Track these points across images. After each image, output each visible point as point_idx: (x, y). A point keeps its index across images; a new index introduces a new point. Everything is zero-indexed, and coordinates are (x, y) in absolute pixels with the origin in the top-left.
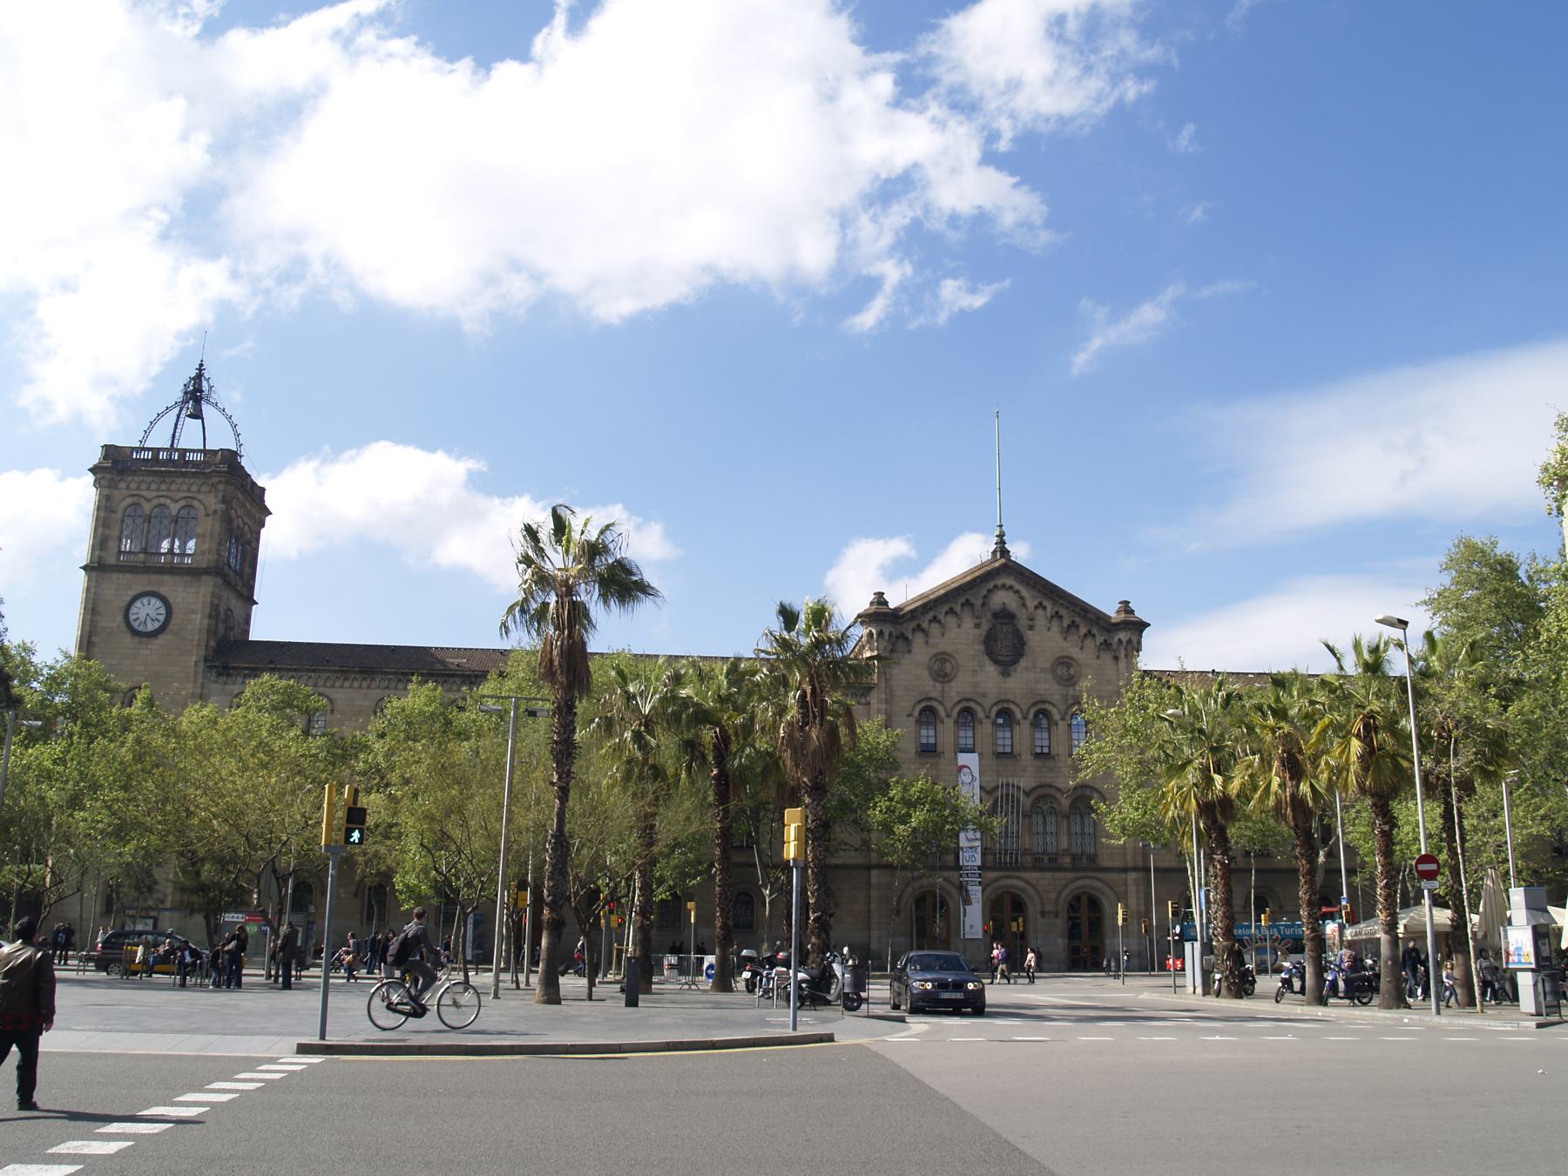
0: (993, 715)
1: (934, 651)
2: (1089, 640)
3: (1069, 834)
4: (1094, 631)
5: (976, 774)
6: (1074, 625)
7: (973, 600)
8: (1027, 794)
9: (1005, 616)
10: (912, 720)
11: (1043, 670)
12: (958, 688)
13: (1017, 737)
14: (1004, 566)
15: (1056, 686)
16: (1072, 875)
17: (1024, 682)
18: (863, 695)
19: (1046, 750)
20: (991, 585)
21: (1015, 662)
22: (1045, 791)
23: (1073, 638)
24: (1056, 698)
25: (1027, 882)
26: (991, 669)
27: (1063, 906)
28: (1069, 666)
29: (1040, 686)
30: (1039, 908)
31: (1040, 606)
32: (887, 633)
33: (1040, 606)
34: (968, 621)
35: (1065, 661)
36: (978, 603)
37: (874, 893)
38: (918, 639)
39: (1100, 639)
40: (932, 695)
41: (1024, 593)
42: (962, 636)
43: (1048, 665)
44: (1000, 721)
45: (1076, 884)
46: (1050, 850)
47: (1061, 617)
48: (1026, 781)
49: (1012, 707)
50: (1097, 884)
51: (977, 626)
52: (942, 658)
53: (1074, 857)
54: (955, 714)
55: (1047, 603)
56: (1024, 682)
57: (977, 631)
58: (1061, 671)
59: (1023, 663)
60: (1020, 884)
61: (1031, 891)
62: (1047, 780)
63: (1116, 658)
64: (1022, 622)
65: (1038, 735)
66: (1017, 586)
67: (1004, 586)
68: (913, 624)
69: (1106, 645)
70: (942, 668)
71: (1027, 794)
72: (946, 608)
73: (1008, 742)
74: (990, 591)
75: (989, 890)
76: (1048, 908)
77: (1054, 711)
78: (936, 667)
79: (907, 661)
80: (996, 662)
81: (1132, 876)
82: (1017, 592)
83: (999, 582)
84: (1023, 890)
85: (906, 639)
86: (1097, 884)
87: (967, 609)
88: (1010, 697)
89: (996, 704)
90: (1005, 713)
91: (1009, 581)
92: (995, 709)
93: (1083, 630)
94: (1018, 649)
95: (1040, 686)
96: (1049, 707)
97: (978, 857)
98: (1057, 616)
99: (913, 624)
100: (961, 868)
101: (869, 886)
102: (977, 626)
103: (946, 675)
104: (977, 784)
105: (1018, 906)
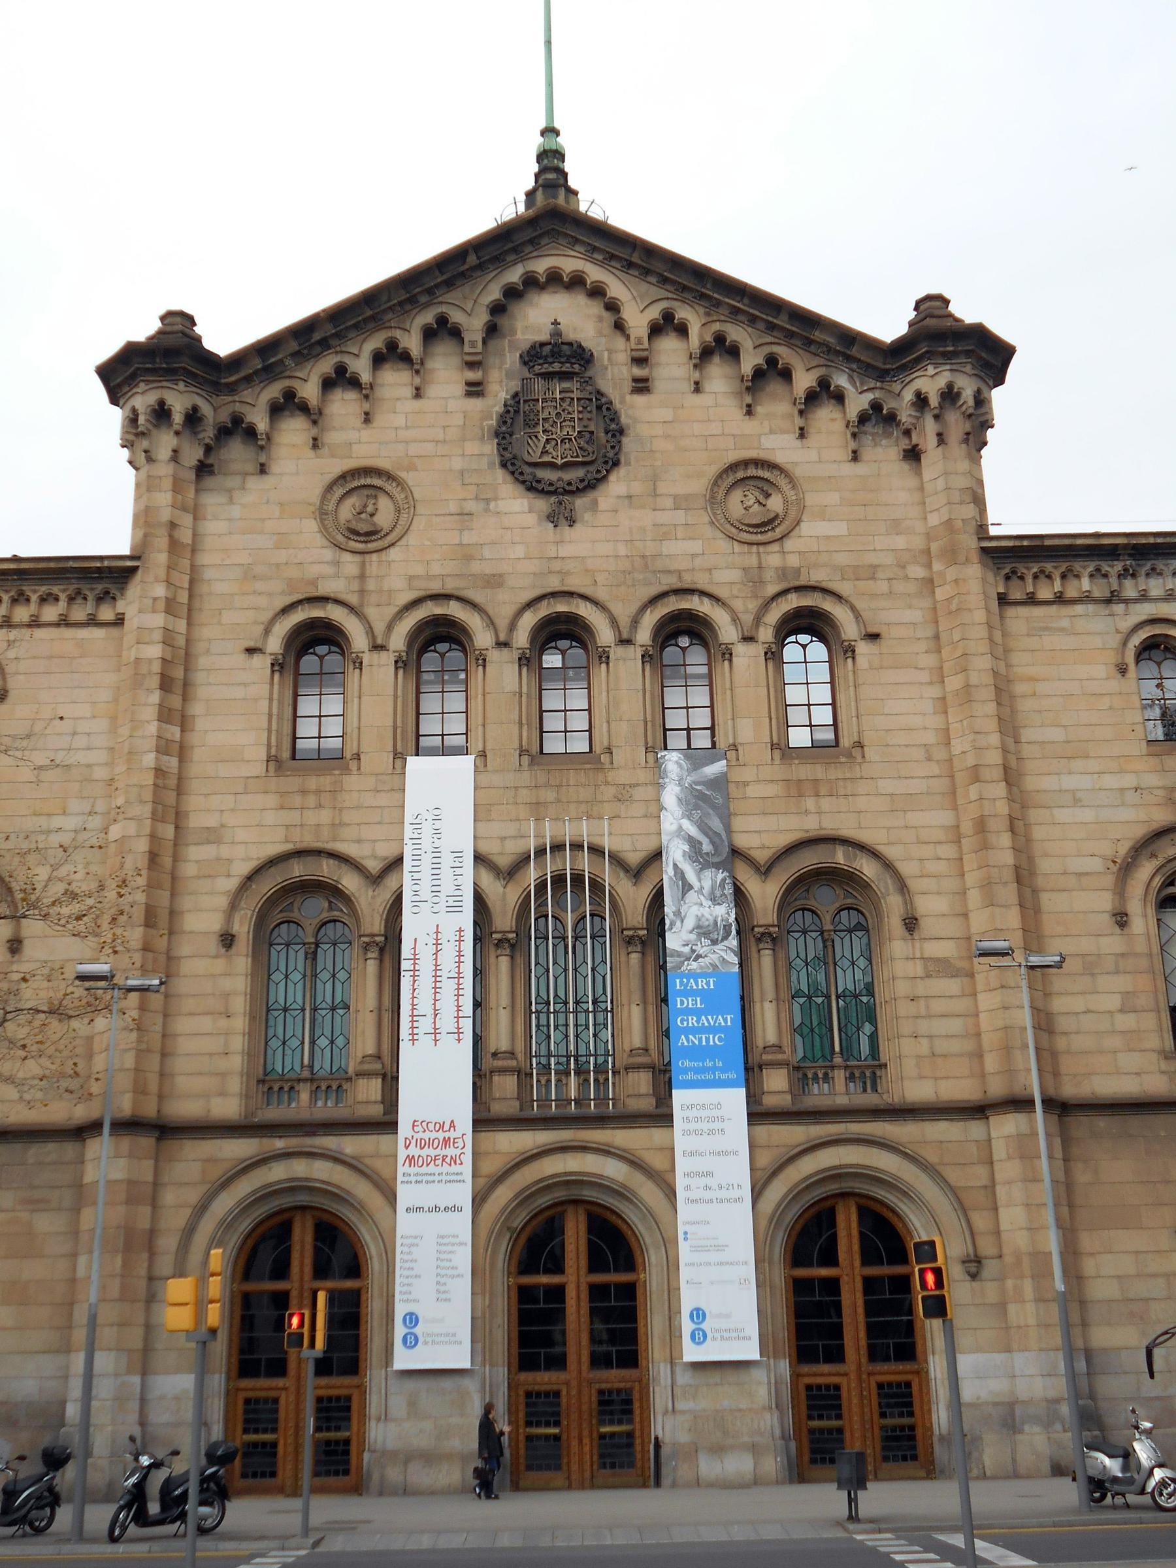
0: (522, 638)
4: (841, 380)
6: (772, 372)
7: (456, 317)
9: (561, 359)
10: (262, 663)
11: (680, 502)
12: (408, 569)
13: (600, 700)
15: (724, 545)
18: (105, 597)
21: (590, 485)
23: (777, 407)
25: (635, 1163)
26: (518, 508)
28: (766, 488)
29: (672, 547)
31: (665, 325)
33: (665, 325)
35: (752, 473)
39: (858, 402)
41: (616, 288)
43: (699, 486)
44: (552, 660)
45: (809, 1165)
47: (733, 352)
49: (584, 610)
51: (475, 389)
52: (365, 481)
54: (398, 641)
57: (475, 404)
58: (739, 504)
59: (617, 485)
60: (613, 1169)
63: (913, 455)
64: (613, 372)
66: (595, 273)
67: (554, 279)
68: (274, 391)
69: (877, 417)
72: (376, 342)
73: (579, 722)
74: (513, 294)
77: (719, 617)
78: (346, 511)
80: (533, 487)
81: (1006, 1126)
82: (597, 292)
83: (541, 266)
85: (251, 433)
88: (575, 583)
89: (530, 604)
91: (569, 263)
92: (529, 620)
93: (804, 380)
95: (672, 547)
96: (703, 606)
98: (720, 348)
99: (274, 391)
101: (80, 1194)
102: (475, 389)
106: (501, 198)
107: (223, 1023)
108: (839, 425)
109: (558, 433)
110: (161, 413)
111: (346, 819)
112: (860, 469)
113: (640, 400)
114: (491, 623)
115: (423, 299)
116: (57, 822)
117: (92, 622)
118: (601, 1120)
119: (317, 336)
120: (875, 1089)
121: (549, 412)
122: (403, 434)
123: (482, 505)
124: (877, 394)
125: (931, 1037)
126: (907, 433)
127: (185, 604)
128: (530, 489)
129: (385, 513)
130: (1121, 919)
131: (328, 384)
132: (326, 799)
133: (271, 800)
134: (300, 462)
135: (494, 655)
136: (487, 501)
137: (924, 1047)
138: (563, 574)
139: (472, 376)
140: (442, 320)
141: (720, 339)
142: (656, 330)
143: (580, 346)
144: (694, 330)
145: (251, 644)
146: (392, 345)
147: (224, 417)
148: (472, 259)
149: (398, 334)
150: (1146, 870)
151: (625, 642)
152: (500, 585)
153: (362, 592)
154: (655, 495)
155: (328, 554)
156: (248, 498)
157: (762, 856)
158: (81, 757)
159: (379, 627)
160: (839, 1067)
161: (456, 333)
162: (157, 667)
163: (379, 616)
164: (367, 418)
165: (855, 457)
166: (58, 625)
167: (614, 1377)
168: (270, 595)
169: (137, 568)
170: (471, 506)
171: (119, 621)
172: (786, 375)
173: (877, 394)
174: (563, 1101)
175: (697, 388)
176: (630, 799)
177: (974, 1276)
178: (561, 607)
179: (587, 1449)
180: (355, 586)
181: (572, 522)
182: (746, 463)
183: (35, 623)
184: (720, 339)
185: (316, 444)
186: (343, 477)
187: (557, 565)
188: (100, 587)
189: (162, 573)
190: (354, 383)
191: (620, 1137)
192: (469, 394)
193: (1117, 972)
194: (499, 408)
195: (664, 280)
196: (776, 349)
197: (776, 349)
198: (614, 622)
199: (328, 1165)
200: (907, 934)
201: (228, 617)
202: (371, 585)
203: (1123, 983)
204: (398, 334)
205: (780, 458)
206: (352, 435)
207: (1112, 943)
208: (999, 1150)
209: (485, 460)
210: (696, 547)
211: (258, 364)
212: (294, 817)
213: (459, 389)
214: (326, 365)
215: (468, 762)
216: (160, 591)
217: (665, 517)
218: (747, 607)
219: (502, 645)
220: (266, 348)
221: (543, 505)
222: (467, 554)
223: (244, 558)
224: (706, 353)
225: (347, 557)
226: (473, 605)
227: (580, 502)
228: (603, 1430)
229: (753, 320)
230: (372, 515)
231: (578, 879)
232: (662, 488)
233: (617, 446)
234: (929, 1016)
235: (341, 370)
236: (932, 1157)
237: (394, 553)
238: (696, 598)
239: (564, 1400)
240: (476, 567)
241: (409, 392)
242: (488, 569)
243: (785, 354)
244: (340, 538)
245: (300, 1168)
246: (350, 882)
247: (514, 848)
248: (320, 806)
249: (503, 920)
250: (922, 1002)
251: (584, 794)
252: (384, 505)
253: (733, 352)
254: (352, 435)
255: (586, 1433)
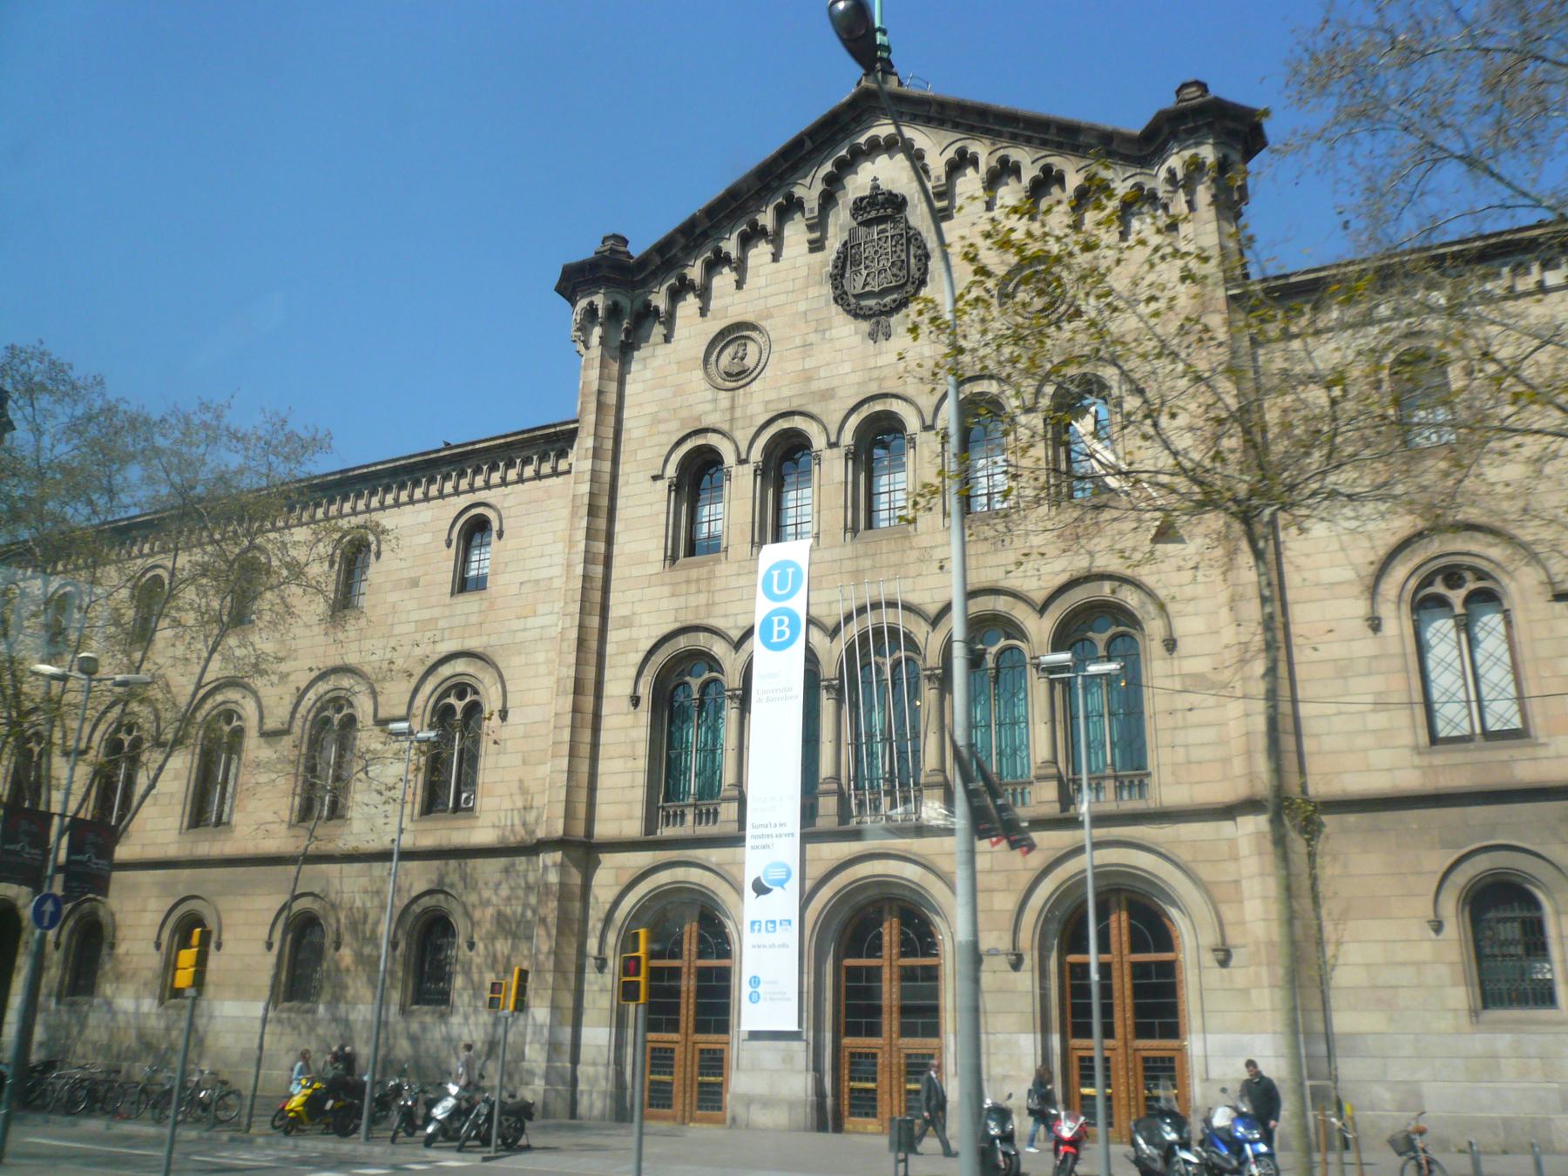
9: (883, 207)
10: (663, 485)
26: (847, 331)
30: (1209, 937)
35: (1035, 269)
47: (1013, 170)
49: (896, 406)
51: (816, 246)
52: (735, 333)
57: (818, 256)
60: (910, 872)
80: (857, 314)
107: (631, 764)
109: (876, 267)
110: (591, 311)
111: (717, 599)
115: (775, 184)
116: (531, 622)
117: (555, 473)
119: (698, 231)
120: (1141, 795)
121: (870, 251)
122: (764, 292)
123: (820, 335)
124: (1138, 179)
125: (1186, 746)
126: (1165, 207)
127: (611, 450)
128: (856, 316)
130: (1375, 624)
132: (703, 585)
133: (666, 590)
134: (692, 327)
136: (824, 331)
137: (1180, 755)
138: (881, 380)
143: (890, 193)
145: (655, 473)
147: (638, 304)
148: (808, 144)
150: (1400, 572)
152: (833, 397)
153: (732, 420)
155: (709, 395)
156: (657, 362)
157: (1039, 597)
158: (544, 574)
159: (743, 447)
160: (1108, 777)
162: (586, 500)
166: (533, 479)
167: (1155, 1046)
168: (668, 432)
169: (576, 429)
170: (813, 338)
172: (1060, 180)
173: (1138, 179)
176: (931, 559)
177: (1224, 963)
178: (878, 407)
179: (896, 1102)
180: (728, 417)
181: (888, 336)
183: (521, 480)
186: (722, 334)
187: (875, 374)
188: (557, 446)
189: (592, 430)
192: (812, 250)
193: (1369, 674)
194: (834, 256)
196: (1050, 160)
197: (1050, 160)
199: (699, 871)
200: (1166, 654)
201: (641, 455)
202: (738, 413)
203: (1377, 683)
206: (728, 300)
207: (1366, 645)
209: (823, 300)
211: (658, 260)
212: (681, 601)
220: (663, 247)
221: (865, 326)
223: (652, 408)
225: (723, 394)
228: (910, 1086)
230: (742, 359)
234: (1184, 727)
236: (1184, 855)
238: (986, 382)
239: (880, 1061)
240: (815, 386)
242: (823, 385)
243: (1057, 162)
244: (719, 380)
245: (680, 874)
246: (719, 649)
247: (840, 611)
248: (699, 591)
249: (828, 670)
250: (1180, 715)
251: (894, 558)
252: (752, 348)
254: (728, 300)
255: (895, 1089)
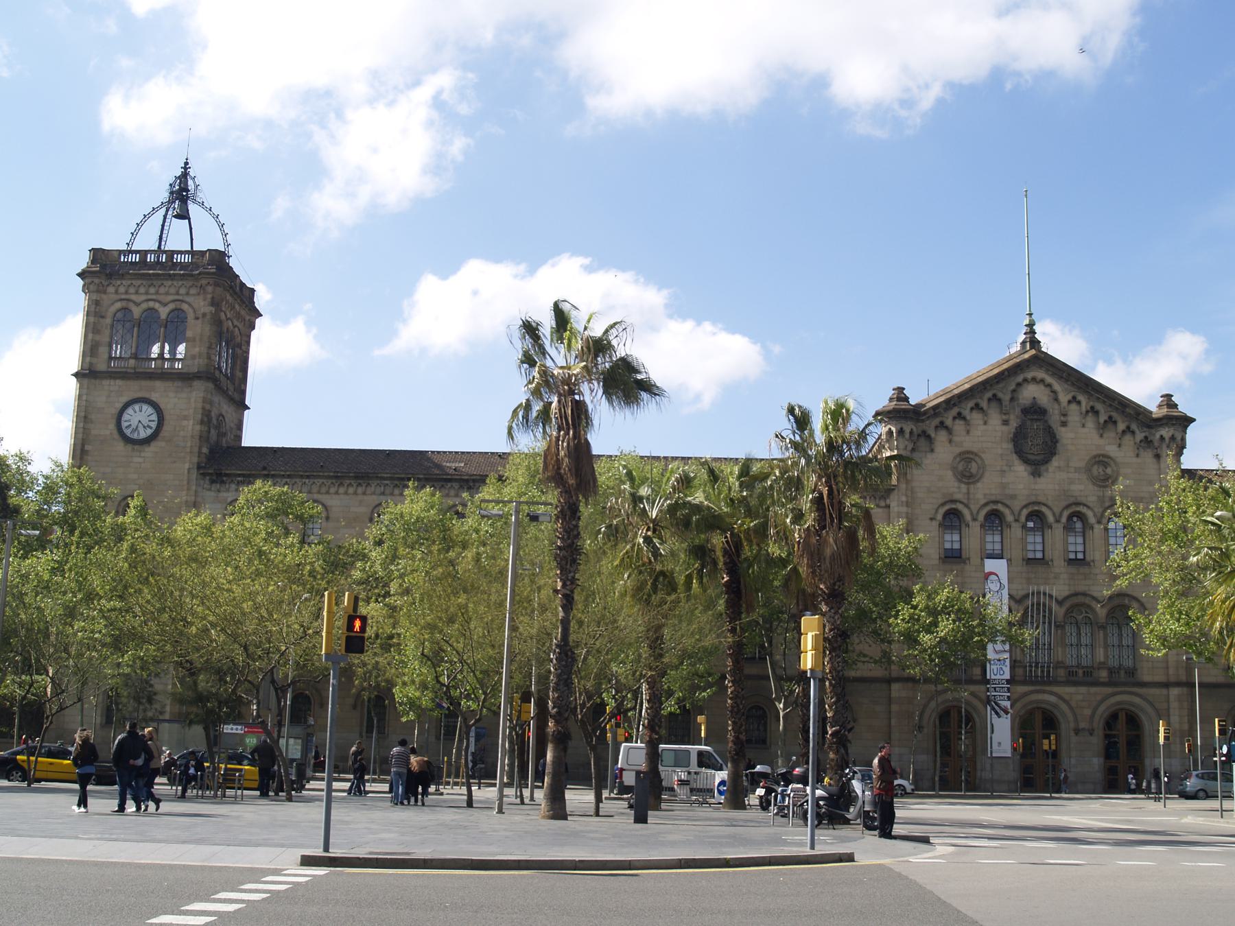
0: (1023, 519)
1: (958, 450)
2: (1128, 437)
3: (1106, 646)
4: (1134, 427)
5: (1005, 581)
6: (1111, 421)
7: (1000, 395)
8: (1060, 603)
9: (1035, 412)
10: (935, 524)
11: (1077, 470)
12: (984, 490)
13: (1049, 542)
14: (1034, 357)
15: (1091, 487)
16: (1109, 690)
17: (1059, 482)
19: (1080, 556)
20: (1020, 379)
21: (1046, 461)
22: (1081, 599)
23: (1110, 434)
24: (1092, 500)
26: (1021, 469)
27: (1099, 724)
28: (1106, 465)
29: (1073, 487)
30: (1072, 725)
31: (1074, 400)
32: (907, 430)
33: (1074, 400)
34: (995, 419)
35: (1102, 460)
36: (1006, 398)
37: (894, 708)
38: (941, 437)
39: (1140, 436)
40: (958, 496)
41: (1057, 386)
42: (989, 434)
43: (1082, 464)
44: (1031, 524)
45: (1113, 700)
46: (1084, 663)
47: (1097, 413)
48: (1059, 589)
49: (1044, 509)
50: (1137, 700)
52: (967, 457)
53: (1111, 671)
54: (981, 517)
55: (1080, 397)
56: (1059, 482)
57: (1005, 428)
58: (1096, 470)
59: (1055, 462)
60: (1053, 699)
61: (1064, 706)
62: (1081, 589)
63: (1158, 457)
64: (1054, 418)
65: (1071, 539)
66: (1049, 379)
67: (1034, 379)
68: (936, 421)
69: (1147, 442)
70: (968, 468)
71: (1060, 603)
72: (971, 404)
73: (1039, 547)
74: (1019, 385)
75: (1018, 705)
76: (1082, 725)
77: (1090, 514)
78: (960, 467)
79: (929, 460)
80: (1026, 461)
81: (1174, 692)
82: (1049, 385)
83: (1029, 375)
84: (1055, 706)
85: (928, 437)
86: (1137, 700)
87: (994, 404)
88: (1041, 499)
89: (1025, 506)
90: (1036, 516)
91: (1040, 374)
92: (1025, 512)
93: (1121, 426)
94: (1051, 447)
95: (1073, 487)
97: (1007, 670)
98: (1093, 411)
99: (936, 421)
100: (988, 682)
101: (890, 700)
102: (1006, 422)
103: (971, 476)
104: (1005, 593)
105: (1050, 723)
106: (1012, 346)
108: (1132, 443)
112: (1139, 460)
113: (1063, 429)
114: (1013, 513)
118: (1050, 683)
129: (974, 467)
131: (954, 418)
135: (1014, 524)
139: (1004, 417)
140: (994, 395)
141: (1092, 408)
142: (1069, 402)
144: (1084, 404)
146: (977, 405)
149: (979, 401)
151: (1058, 521)
154: (1068, 466)
155: (956, 484)
161: (999, 400)
163: (974, 508)
164: (968, 432)
165: (1138, 456)
170: (1005, 468)
171: (888, 507)
172: (1115, 423)
174: (1036, 676)
175: (1083, 426)
181: (1039, 476)
182: (1099, 456)
184: (1092, 408)
185: (950, 441)
186: (960, 454)
190: (964, 418)
191: (1056, 689)
195: (1073, 384)
198: (1054, 514)
204: (979, 401)
205: (1112, 454)
208: (1172, 698)
210: (1082, 487)
213: (999, 422)
214: (954, 412)
215: (1004, 562)
216: (904, 499)
217: (1071, 475)
218: (1098, 510)
219: (1017, 521)
221: (1029, 468)
222: (1003, 486)
224: (1087, 412)
226: (1007, 506)
227: (1043, 468)
229: (1104, 402)
231: (1044, 605)
232: (1071, 464)
233: (1055, 448)
235: (959, 414)
237: (979, 485)
241: (981, 422)
243: (1114, 414)
247: (1021, 593)
253: (1097, 413)
